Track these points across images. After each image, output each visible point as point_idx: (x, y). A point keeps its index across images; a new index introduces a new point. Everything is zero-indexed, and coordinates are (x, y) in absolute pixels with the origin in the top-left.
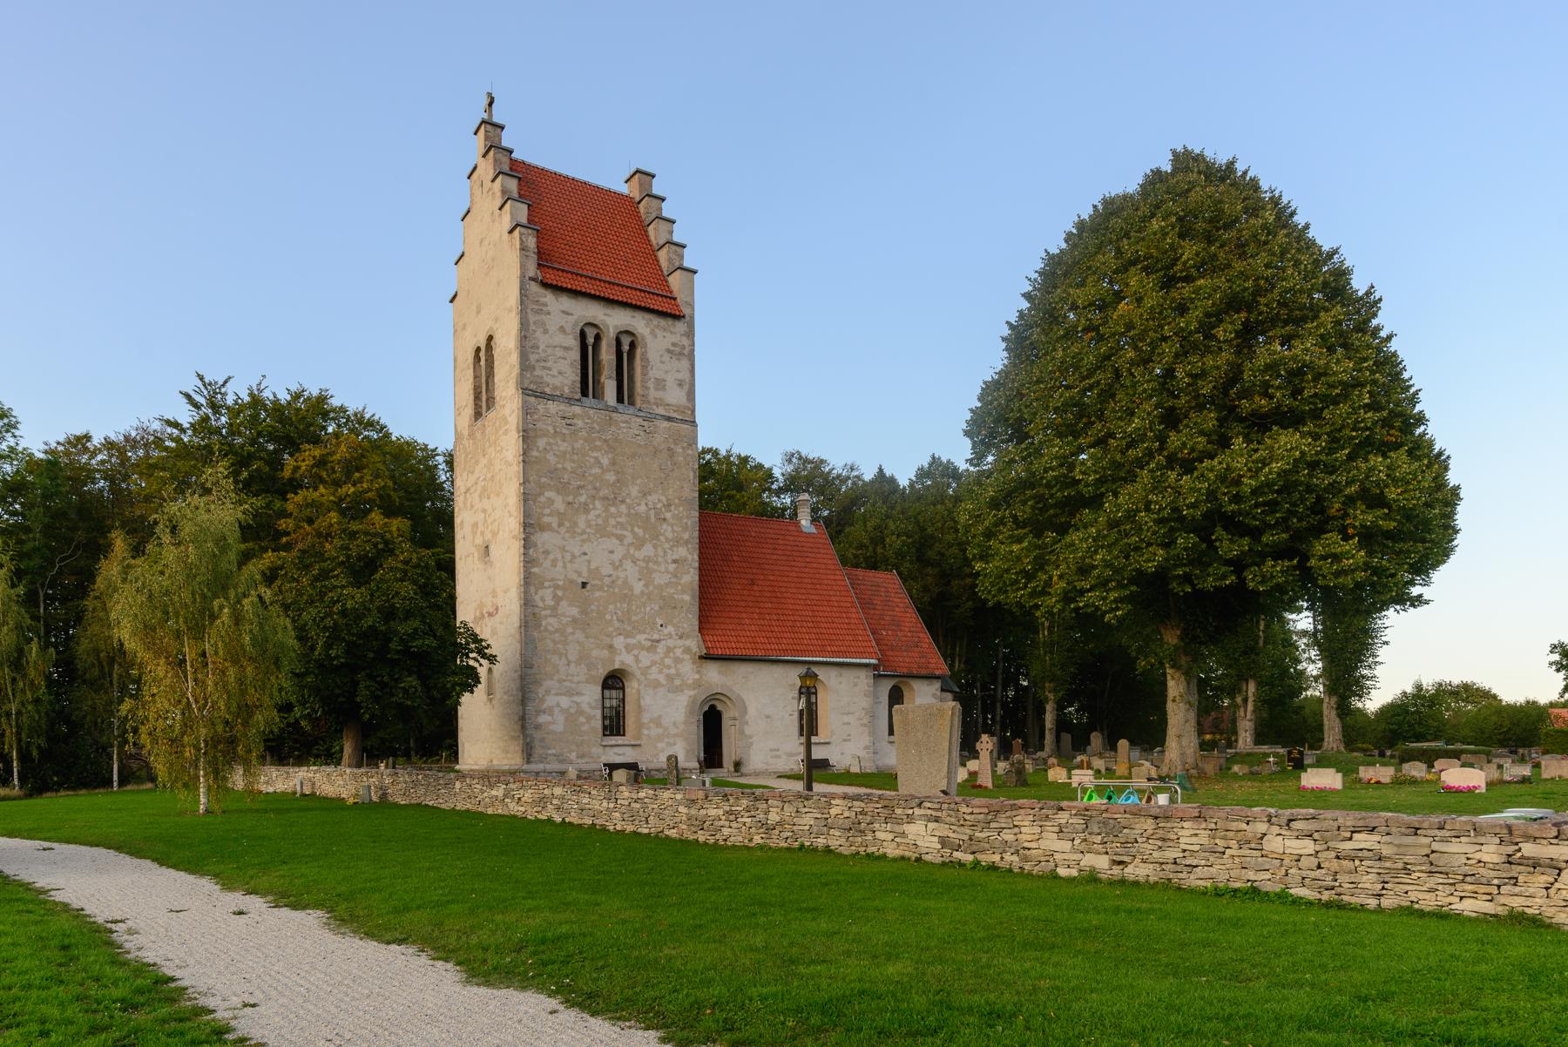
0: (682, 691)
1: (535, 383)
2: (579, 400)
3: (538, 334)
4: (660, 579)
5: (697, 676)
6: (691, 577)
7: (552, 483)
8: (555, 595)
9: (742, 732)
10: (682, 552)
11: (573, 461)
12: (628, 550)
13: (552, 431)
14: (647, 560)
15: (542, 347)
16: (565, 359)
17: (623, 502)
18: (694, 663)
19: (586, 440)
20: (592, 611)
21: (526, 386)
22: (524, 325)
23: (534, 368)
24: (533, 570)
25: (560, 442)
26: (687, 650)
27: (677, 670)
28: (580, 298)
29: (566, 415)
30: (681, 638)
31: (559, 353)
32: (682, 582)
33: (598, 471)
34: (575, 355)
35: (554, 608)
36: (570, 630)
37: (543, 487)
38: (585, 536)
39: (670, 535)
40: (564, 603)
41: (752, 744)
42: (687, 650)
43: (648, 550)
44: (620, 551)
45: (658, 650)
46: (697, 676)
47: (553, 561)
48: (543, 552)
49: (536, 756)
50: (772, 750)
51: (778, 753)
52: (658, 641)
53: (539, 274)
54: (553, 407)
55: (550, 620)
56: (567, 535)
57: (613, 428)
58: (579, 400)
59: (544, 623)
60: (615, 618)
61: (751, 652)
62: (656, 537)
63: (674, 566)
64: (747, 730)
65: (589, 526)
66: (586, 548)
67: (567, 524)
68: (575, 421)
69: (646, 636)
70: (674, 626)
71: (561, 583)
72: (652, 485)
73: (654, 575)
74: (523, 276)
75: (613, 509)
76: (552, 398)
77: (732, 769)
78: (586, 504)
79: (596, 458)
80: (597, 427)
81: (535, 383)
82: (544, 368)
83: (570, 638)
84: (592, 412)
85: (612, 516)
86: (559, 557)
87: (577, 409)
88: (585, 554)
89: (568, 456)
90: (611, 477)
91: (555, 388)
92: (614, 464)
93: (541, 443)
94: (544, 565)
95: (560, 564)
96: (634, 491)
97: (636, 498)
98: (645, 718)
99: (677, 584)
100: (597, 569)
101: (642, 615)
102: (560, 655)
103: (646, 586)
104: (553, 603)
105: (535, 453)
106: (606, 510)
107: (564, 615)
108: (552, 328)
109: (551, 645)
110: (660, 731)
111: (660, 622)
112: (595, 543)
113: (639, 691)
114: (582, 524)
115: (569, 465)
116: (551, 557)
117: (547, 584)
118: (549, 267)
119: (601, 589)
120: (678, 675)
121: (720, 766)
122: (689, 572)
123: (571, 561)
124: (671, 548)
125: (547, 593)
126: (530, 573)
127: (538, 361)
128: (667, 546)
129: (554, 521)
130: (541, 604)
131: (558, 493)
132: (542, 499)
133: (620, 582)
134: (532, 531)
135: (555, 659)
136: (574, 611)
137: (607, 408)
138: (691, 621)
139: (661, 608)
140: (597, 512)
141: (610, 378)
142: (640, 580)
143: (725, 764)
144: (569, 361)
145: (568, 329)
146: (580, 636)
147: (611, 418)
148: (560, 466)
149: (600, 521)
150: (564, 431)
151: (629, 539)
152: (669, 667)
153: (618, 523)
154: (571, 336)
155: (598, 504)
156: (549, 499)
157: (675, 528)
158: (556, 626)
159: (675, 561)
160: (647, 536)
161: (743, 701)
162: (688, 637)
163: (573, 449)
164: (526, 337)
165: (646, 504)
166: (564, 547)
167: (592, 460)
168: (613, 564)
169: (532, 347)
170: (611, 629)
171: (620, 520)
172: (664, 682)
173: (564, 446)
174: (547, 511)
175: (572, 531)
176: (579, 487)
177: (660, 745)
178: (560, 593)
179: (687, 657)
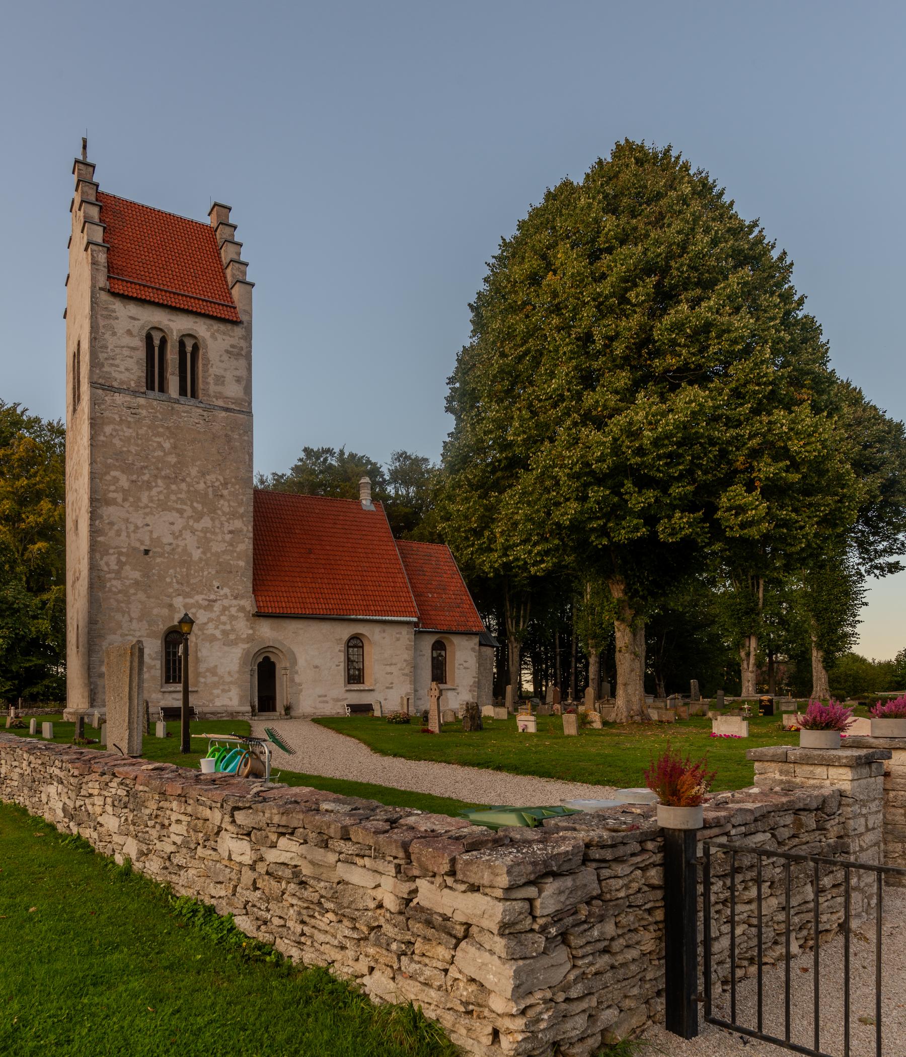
0: (237, 644)
1: (104, 378)
2: (144, 393)
3: (107, 336)
4: (217, 547)
5: (251, 632)
6: (246, 546)
7: (117, 464)
8: (119, 562)
9: (292, 680)
10: (238, 524)
11: (138, 445)
12: (188, 522)
13: (118, 419)
14: (205, 531)
15: (110, 347)
16: (131, 357)
17: (183, 480)
18: (247, 620)
19: (149, 427)
20: (154, 574)
21: (95, 380)
22: (94, 328)
23: (103, 365)
24: (99, 539)
25: (125, 429)
26: (242, 609)
27: (232, 626)
28: (146, 306)
29: (132, 405)
30: (236, 598)
31: (126, 352)
32: (238, 549)
33: (160, 453)
34: (142, 354)
35: (118, 572)
36: (132, 591)
37: (109, 468)
38: (148, 510)
39: (227, 509)
40: (127, 567)
41: (301, 690)
42: (242, 609)
43: (206, 522)
44: (180, 523)
45: (215, 609)
46: (251, 632)
47: (118, 531)
48: (109, 523)
49: (99, 700)
50: (320, 696)
51: (325, 699)
52: (215, 601)
53: (108, 283)
54: (119, 398)
55: (114, 582)
56: (131, 509)
57: (175, 417)
58: (144, 393)
59: (108, 585)
60: (174, 580)
61: (296, 611)
62: (213, 510)
63: (230, 536)
64: (297, 679)
65: (152, 501)
66: (148, 520)
67: (131, 499)
68: (140, 410)
69: (203, 596)
70: (230, 588)
71: (124, 550)
72: (210, 467)
73: (211, 544)
74: (93, 286)
75: (174, 487)
76: (119, 391)
77: (283, 713)
78: (148, 482)
79: (159, 443)
80: (160, 416)
81: (104, 378)
82: (112, 365)
83: (132, 598)
84: (155, 403)
85: (173, 492)
86: (124, 527)
87: (142, 401)
88: (148, 525)
89: (132, 441)
90: (172, 459)
91: (122, 383)
92: (175, 447)
93: (108, 429)
94: (110, 534)
95: (124, 534)
96: (194, 471)
97: (195, 477)
98: (202, 668)
99: (233, 551)
100: (158, 538)
101: (200, 578)
102: (123, 612)
103: (204, 553)
104: (116, 567)
105: (102, 438)
106: (168, 487)
107: (127, 578)
108: (120, 331)
109: (115, 604)
110: (216, 679)
111: (216, 584)
112: (157, 516)
113: (196, 644)
114: (145, 499)
115: (133, 449)
116: (116, 527)
117: (111, 551)
118: (118, 279)
119: (162, 555)
120: (233, 630)
121: (274, 710)
122: (244, 542)
123: (134, 532)
124: (228, 521)
125: (113, 559)
126: (96, 541)
127: (106, 359)
128: (223, 518)
129: (119, 497)
130: (106, 569)
131: (123, 472)
132: (108, 478)
133: (180, 550)
134: (98, 505)
135: (119, 616)
136: (137, 575)
137: (170, 400)
138: (245, 584)
139: (217, 572)
140: (159, 489)
141: (173, 374)
142: (198, 548)
143: (278, 709)
144: (135, 360)
145: (135, 331)
146: (141, 596)
147: (173, 408)
148: (125, 449)
149: (162, 497)
150: (129, 419)
151: (189, 512)
152: (224, 624)
153: (179, 499)
154: (137, 338)
155: (160, 482)
156: (114, 477)
157: (232, 504)
158: (120, 588)
159: (231, 532)
160: (205, 510)
161: (293, 653)
162: (243, 597)
163: (137, 434)
164: (95, 339)
165: (205, 483)
166: (128, 519)
167: (155, 444)
168: (173, 534)
169: (101, 347)
170: (171, 590)
171: (180, 496)
172: (220, 637)
173: (128, 432)
174: (112, 488)
175: (136, 506)
176: (142, 468)
177: (216, 692)
178: (123, 559)
179: (241, 615)
